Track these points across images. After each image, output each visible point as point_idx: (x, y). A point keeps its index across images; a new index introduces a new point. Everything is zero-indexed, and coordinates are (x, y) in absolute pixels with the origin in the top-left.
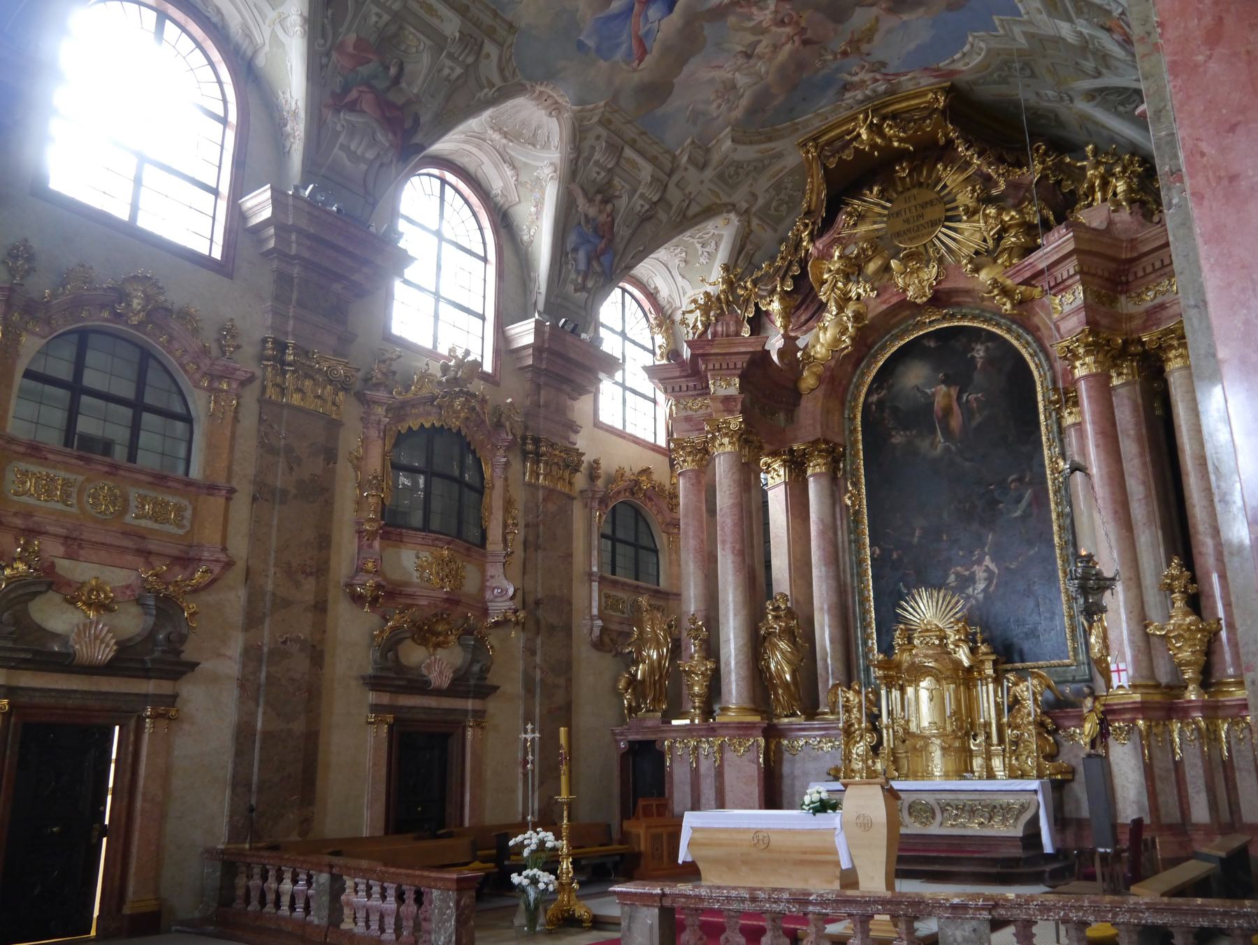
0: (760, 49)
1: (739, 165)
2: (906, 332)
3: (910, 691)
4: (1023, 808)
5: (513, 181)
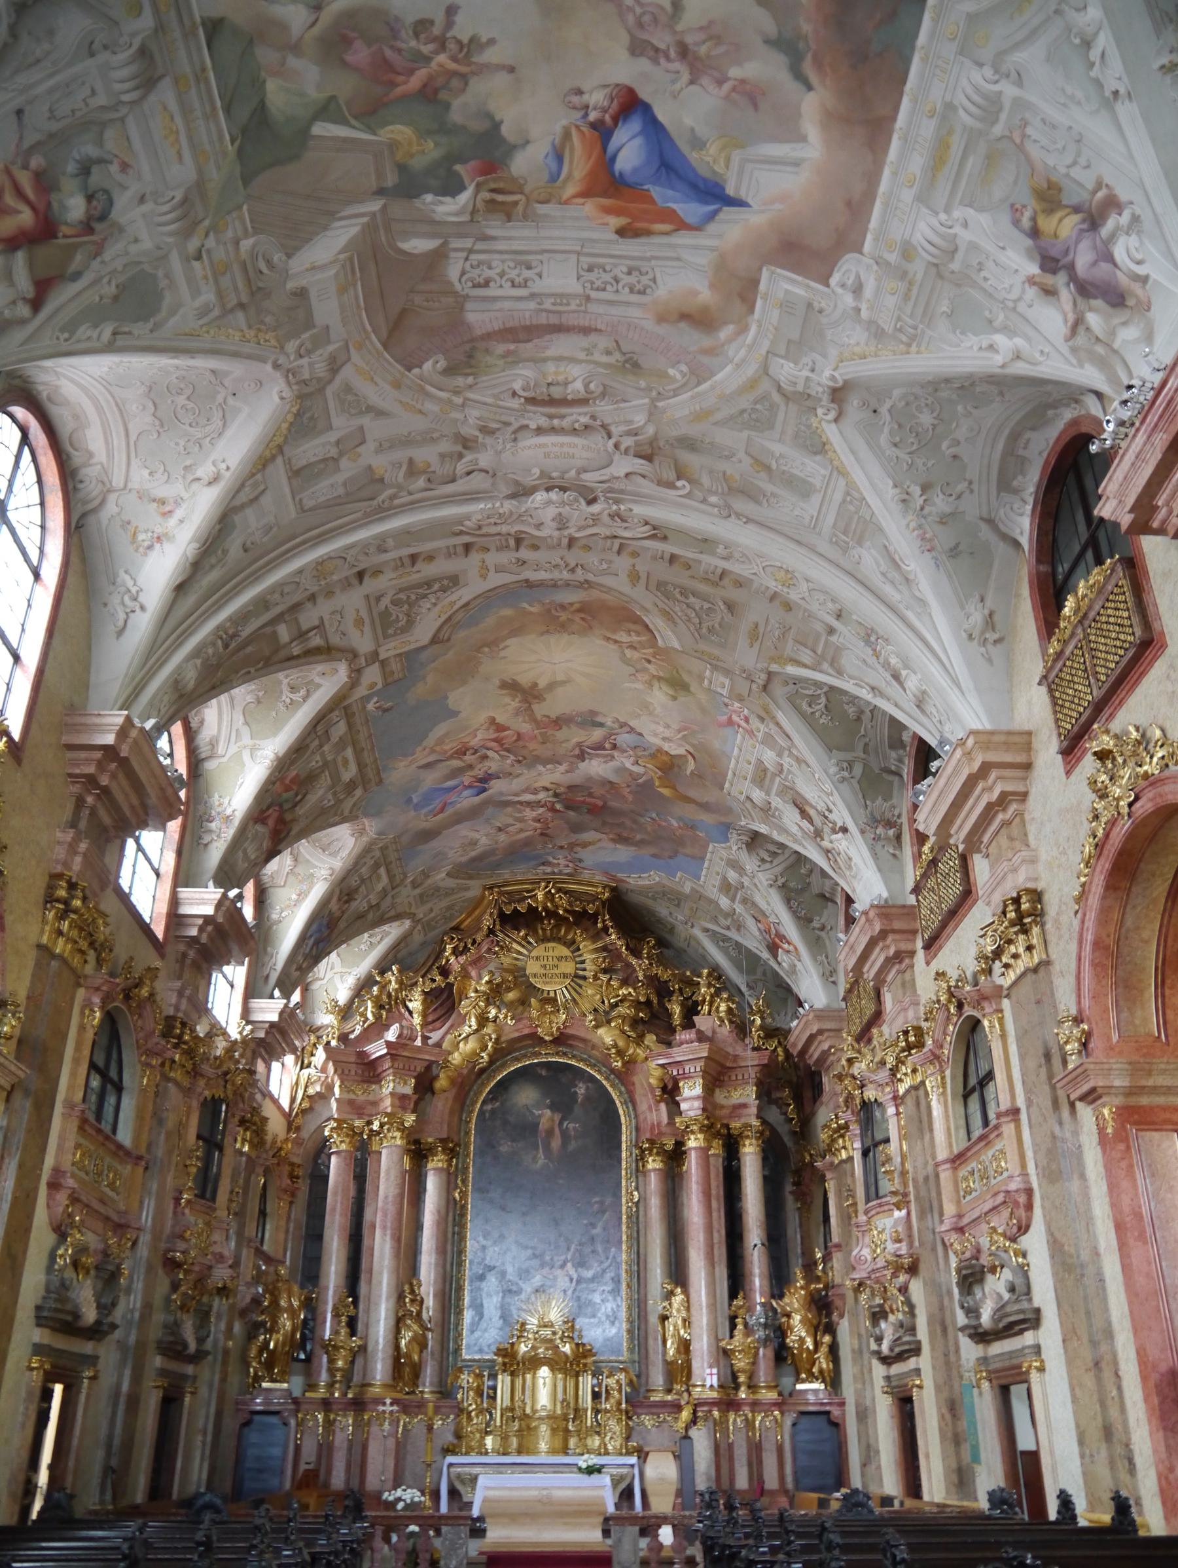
0: (511, 829)
1: (437, 889)
2: (525, 1056)
3: (528, 1376)
4: (622, 1478)
5: (287, 869)
